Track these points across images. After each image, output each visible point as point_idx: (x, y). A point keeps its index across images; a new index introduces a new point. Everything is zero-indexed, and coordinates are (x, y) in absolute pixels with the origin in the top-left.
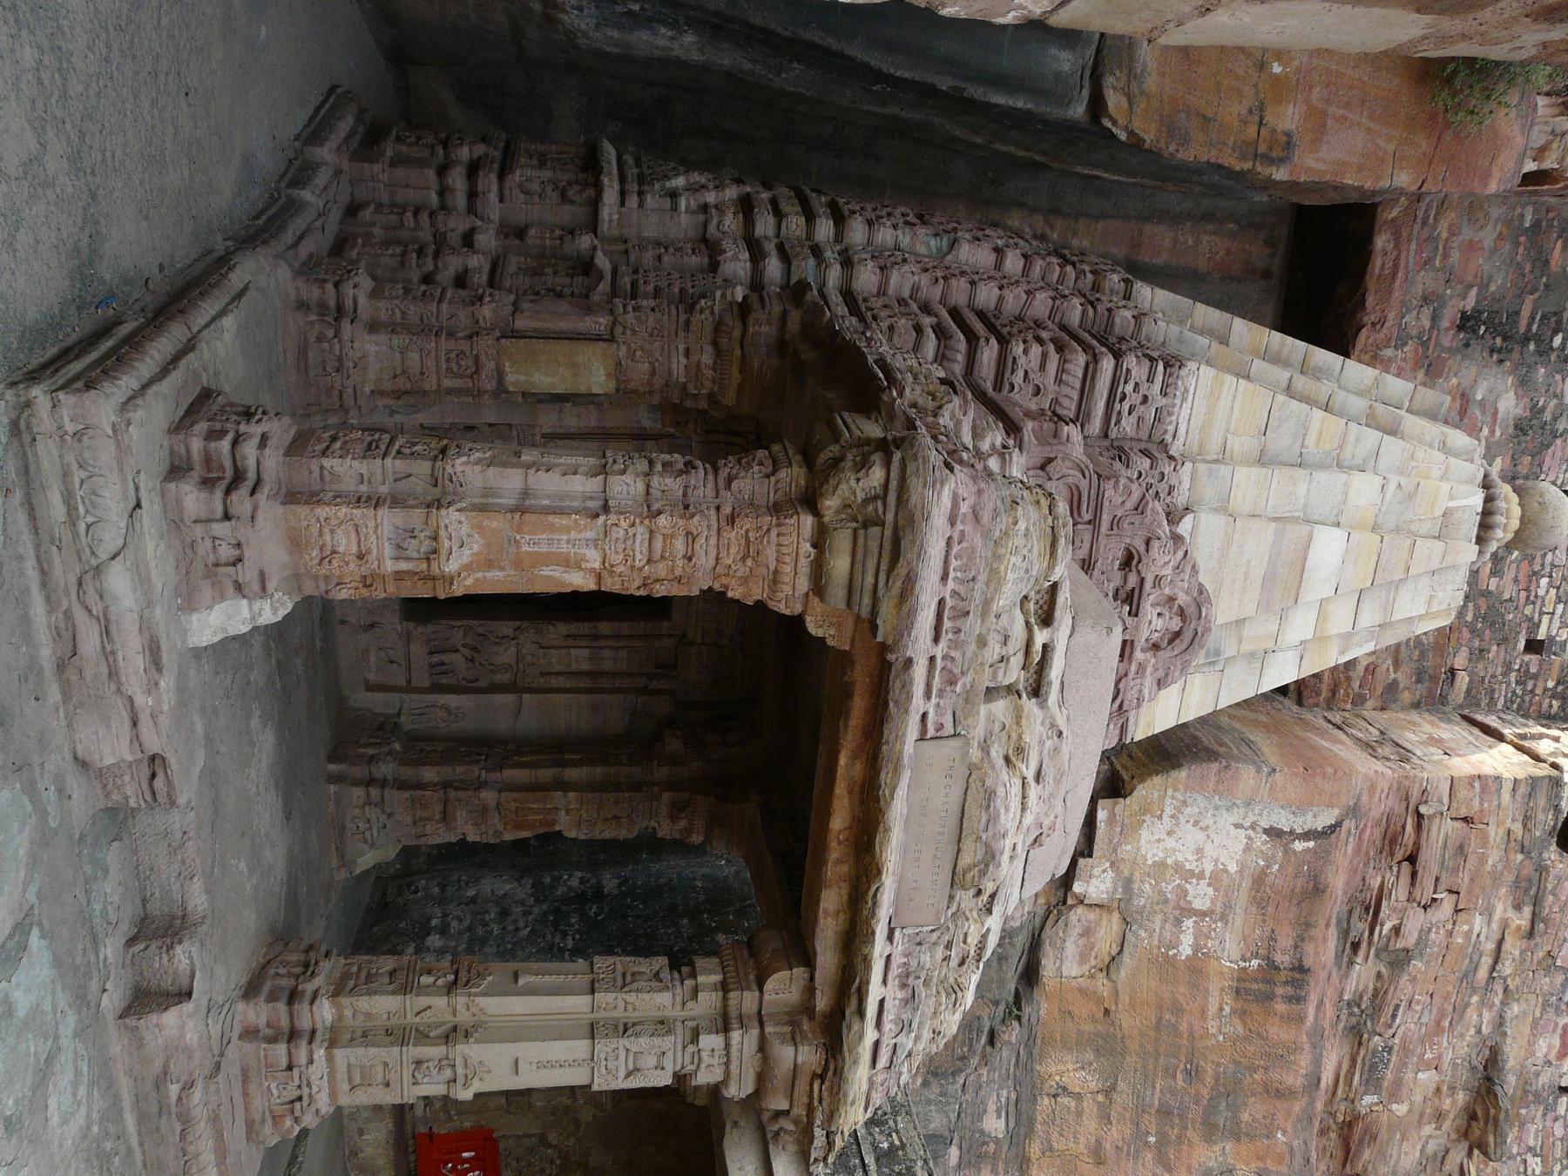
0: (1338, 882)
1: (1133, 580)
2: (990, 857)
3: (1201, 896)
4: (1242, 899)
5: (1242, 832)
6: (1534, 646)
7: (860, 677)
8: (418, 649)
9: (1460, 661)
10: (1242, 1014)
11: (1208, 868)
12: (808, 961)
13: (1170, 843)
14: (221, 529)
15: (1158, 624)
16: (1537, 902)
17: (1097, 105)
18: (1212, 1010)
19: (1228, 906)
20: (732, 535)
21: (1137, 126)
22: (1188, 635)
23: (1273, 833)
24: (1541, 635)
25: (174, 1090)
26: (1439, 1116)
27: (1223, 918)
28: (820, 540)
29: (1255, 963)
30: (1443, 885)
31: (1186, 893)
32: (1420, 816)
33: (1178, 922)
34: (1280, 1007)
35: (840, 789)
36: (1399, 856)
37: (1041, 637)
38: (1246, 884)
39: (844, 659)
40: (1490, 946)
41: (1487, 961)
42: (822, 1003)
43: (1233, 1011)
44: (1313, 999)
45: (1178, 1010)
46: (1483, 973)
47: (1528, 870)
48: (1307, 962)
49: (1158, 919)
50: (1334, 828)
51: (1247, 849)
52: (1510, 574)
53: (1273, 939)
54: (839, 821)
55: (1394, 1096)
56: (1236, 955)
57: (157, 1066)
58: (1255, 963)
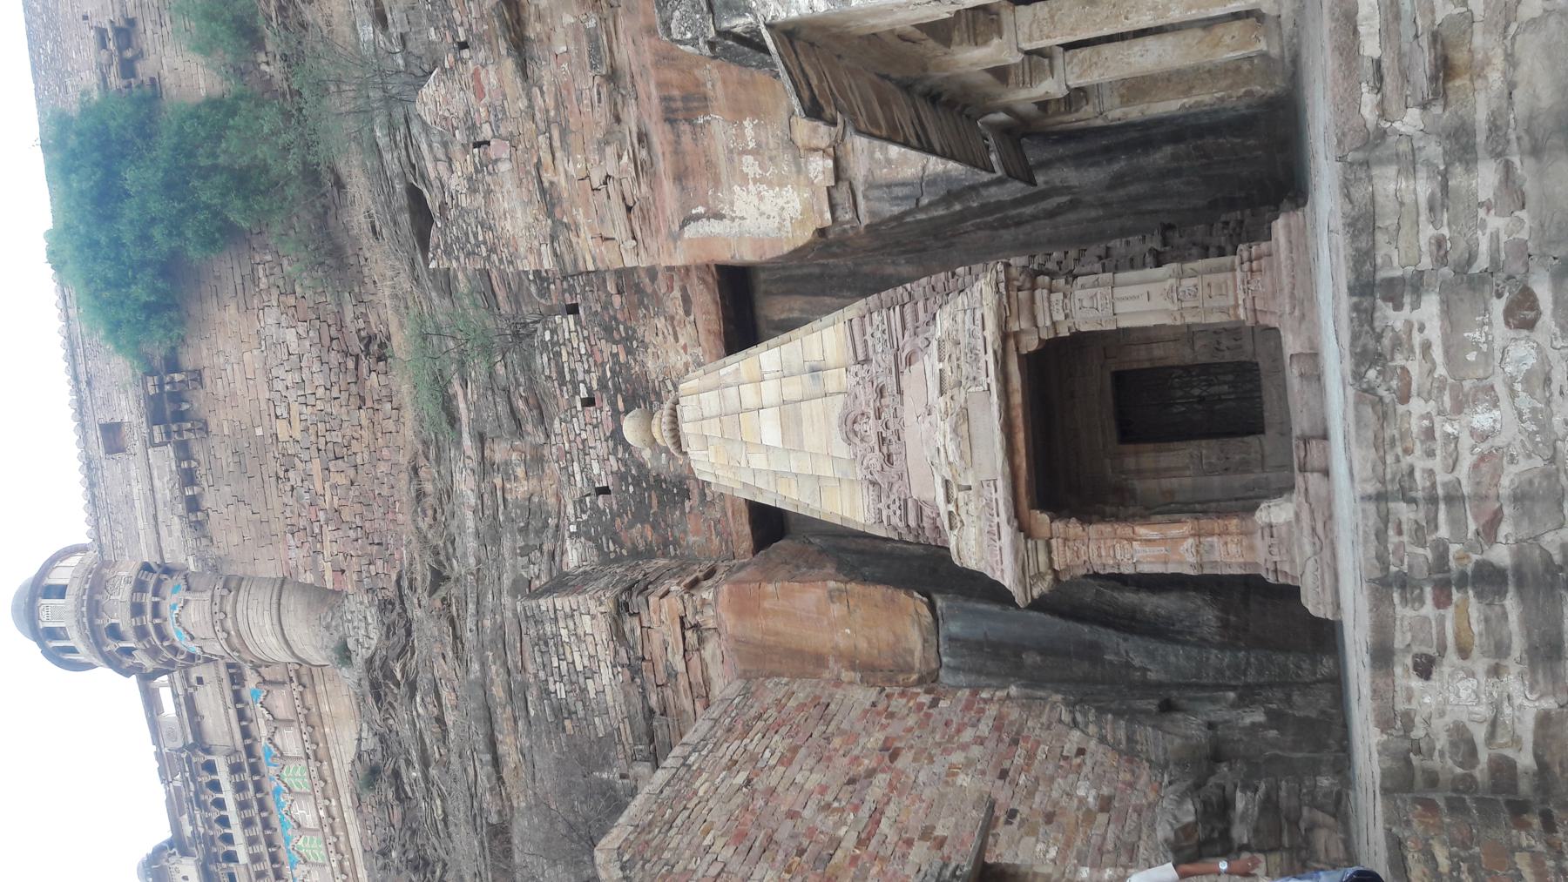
0: (668, 187)
1: (885, 450)
2: (955, 431)
3: (750, 165)
4: (723, 166)
5: (738, 214)
6: (573, 309)
7: (1024, 502)
8: (1248, 348)
9: (617, 300)
10: (698, 84)
11: (751, 186)
12: (1020, 356)
13: (781, 202)
14: (1277, 558)
15: (866, 427)
16: (543, 191)
17: (932, 607)
18: (719, 84)
19: (731, 160)
20: (1085, 558)
21: (911, 601)
22: (849, 422)
23: (719, 216)
24: (571, 317)
25: (1297, 313)
26: (540, 17)
27: (731, 151)
28: (1051, 560)
29: (701, 121)
30: (603, 192)
31: (761, 167)
32: (634, 238)
33: (759, 145)
34: (676, 93)
35: (1023, 452)
36: (636, 209)
37: (952, 508)
38: (724, 178)
39: (1032, 507)
40: (558, 154)
41: (557, 143)
42: (1012, 343)
43: (704, 85)
44: (655, 101)
45: (741, 83)
46: (556, 134)
47: (558, 214)
48: (667, 127)
49: (772, 145)
50: (682, 227)
51: (732, 203)
52: (606, 355)
53: (695, 140)
54: (1020, 437)
55: (575, 27)
56: (714, 123)
57: (1303, 327)
58: (701, 121)
